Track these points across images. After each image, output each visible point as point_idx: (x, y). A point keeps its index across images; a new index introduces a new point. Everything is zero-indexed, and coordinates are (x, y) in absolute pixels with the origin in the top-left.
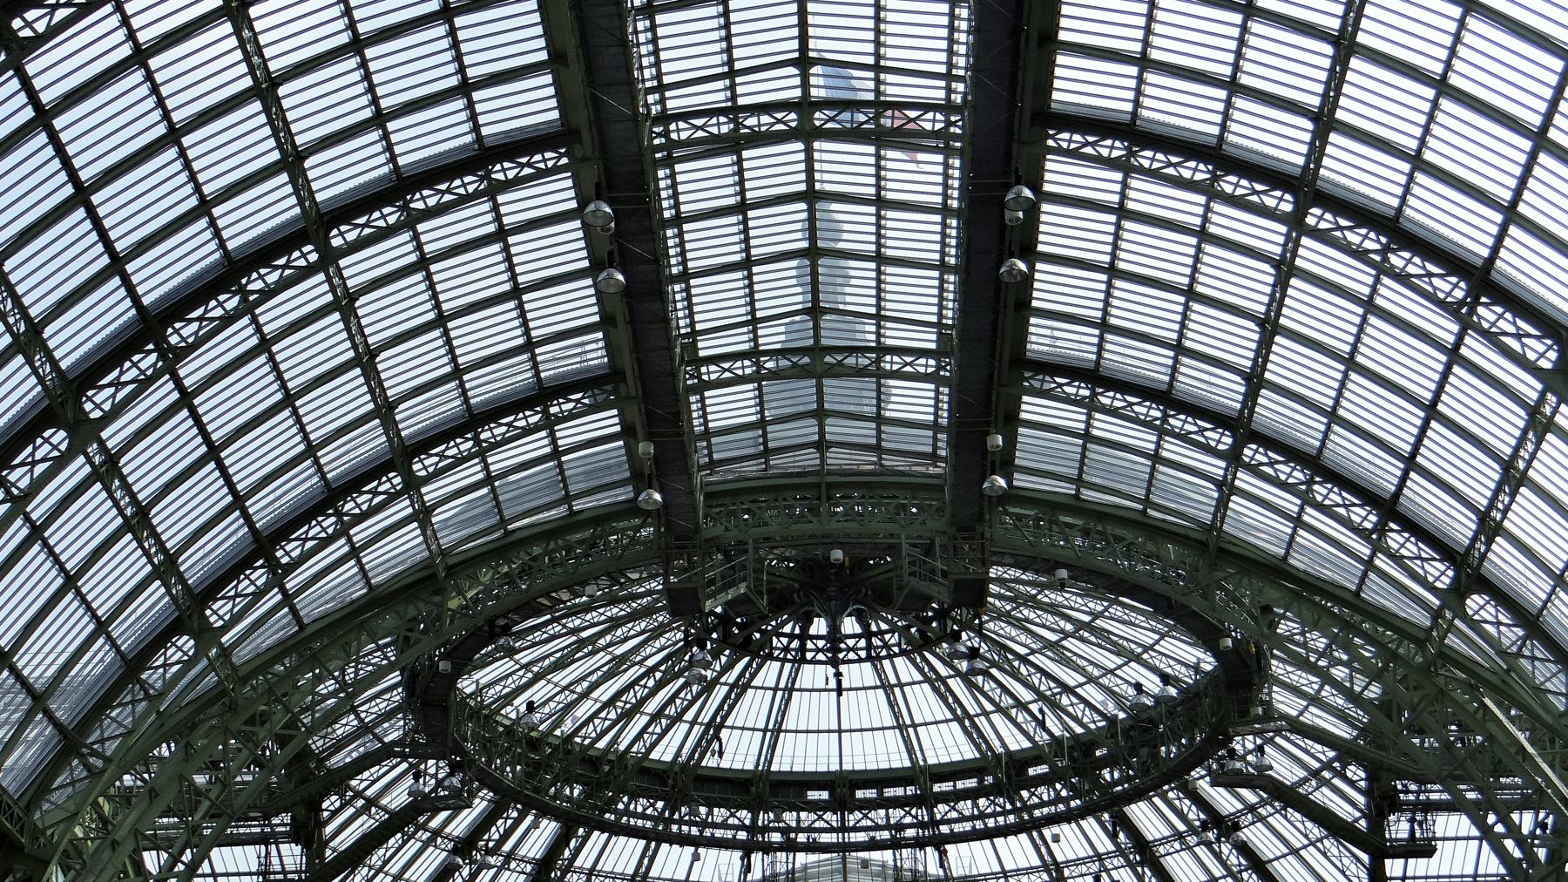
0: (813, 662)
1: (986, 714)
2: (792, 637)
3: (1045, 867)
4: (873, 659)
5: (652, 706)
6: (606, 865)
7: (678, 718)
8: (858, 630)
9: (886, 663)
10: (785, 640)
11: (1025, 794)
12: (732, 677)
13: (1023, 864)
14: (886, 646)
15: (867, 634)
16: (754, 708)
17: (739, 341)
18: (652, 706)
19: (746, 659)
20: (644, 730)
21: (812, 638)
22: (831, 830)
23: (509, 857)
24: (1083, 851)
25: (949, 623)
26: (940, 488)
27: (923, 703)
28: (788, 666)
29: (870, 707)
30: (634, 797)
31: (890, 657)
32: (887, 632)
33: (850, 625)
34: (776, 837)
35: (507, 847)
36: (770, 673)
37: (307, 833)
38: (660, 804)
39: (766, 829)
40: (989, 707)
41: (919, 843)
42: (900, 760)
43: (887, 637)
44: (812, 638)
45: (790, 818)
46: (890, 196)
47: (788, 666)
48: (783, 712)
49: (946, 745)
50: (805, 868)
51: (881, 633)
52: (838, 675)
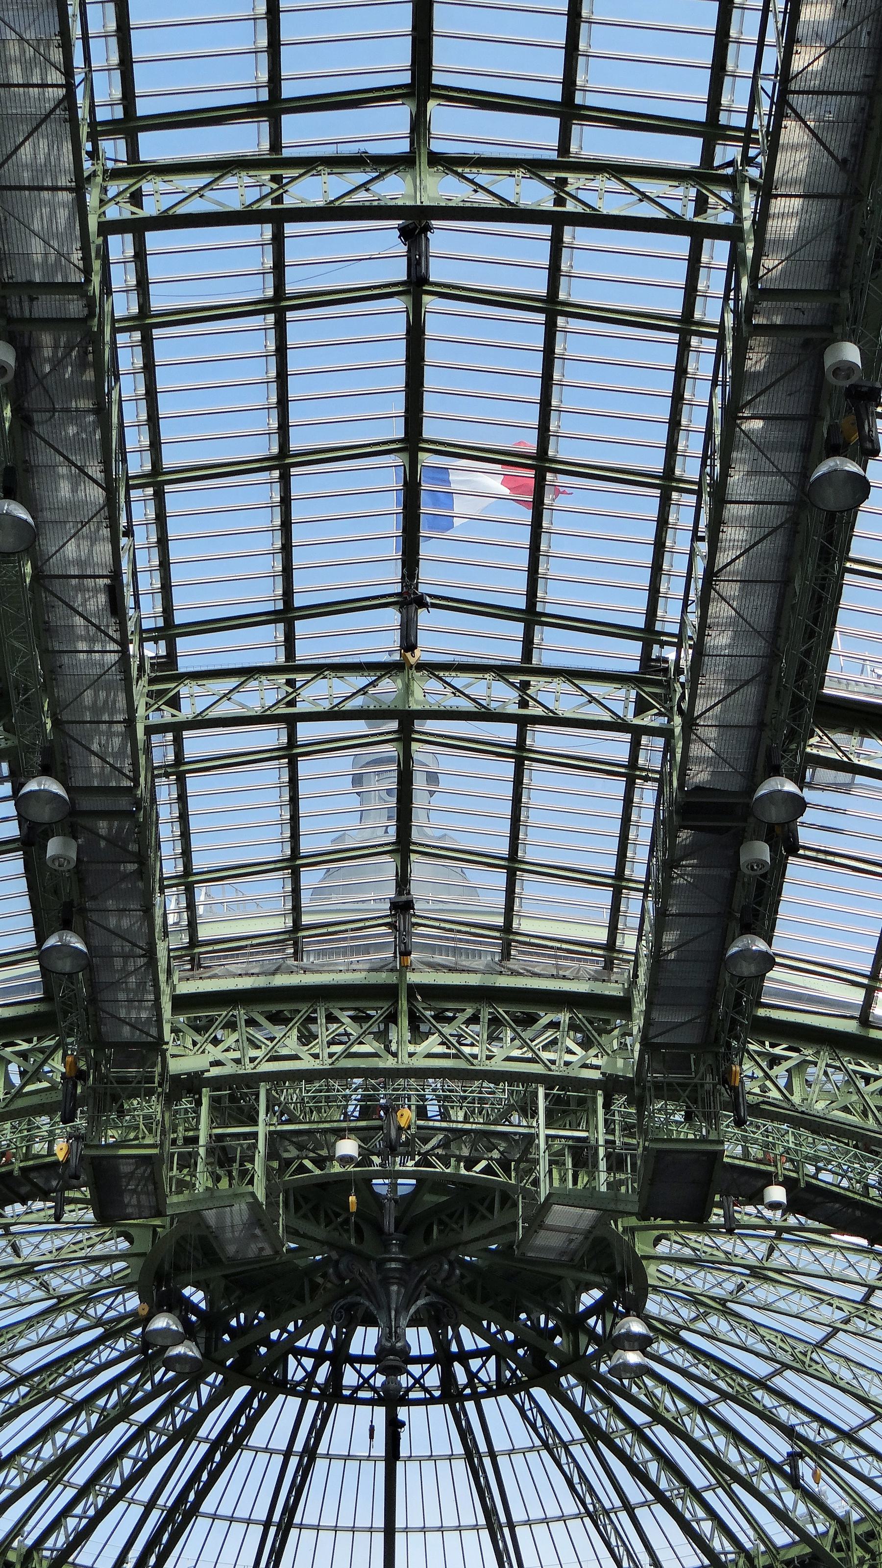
0: (353, 1400)
2: (319, 1356)
4: (449, 1394)
5: (81, 1473)
7: (120, 1494)
8: (428, 1349)
9: (470, 1406)
10: (308, 1362)
12: (212, 1426)
14: (472, 1376)
15: (443, 1357)
17: (261, 645)
18: (82, 1472)
19: (242, 1392)
20: (67, 1511)
21: (355, 1360)
25: (583, 1339)
26: (623, 1006)
28: (312, 1405)
31: (477, 1398)
32: (477, 1353)
33: (420, 1340)
36: (280, 1419)
40: (635, 1492)
44: (355, 1360)
47: (312, 1405)
48: (298, 1489)
51: (464, 1357)
52: (394, 1427)
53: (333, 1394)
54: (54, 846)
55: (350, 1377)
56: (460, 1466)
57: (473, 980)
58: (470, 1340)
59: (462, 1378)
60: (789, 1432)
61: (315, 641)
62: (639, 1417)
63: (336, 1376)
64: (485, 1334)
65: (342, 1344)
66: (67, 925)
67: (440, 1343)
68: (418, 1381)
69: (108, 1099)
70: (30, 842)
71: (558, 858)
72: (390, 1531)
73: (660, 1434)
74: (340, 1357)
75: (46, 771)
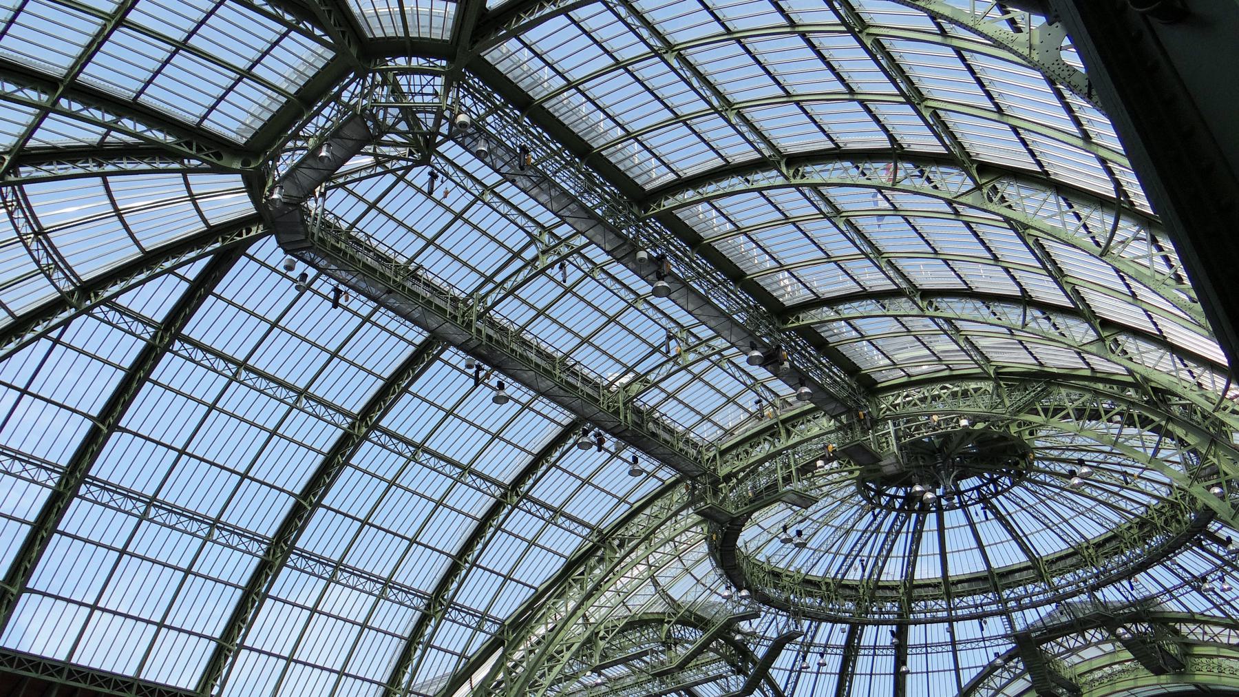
34: (1013, 604)
36: (954, 518)
45: (1020, 590)
50: (1049, 615)
57: (797, 411)
68: (970, 499)
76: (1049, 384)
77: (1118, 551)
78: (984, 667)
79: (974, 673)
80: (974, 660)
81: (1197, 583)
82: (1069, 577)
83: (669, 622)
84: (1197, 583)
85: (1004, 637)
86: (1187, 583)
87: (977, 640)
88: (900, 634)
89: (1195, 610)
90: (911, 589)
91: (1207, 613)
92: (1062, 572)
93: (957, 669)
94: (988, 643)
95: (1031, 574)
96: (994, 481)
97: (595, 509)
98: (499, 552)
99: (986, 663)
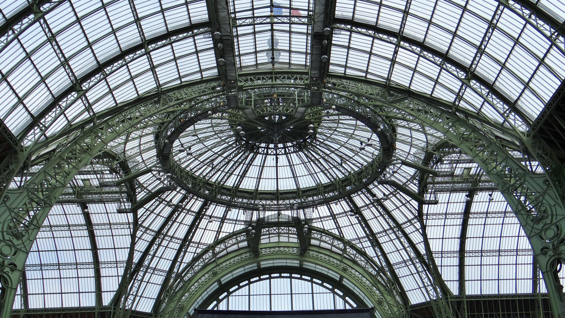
1: (316, 173)
2: (265, 148)
3: (331, 216)
4: (286, 153)
6: (215, 214)
10: (263, 149)
11: (326, 195)
13: (325, 215)
15: (285, 148)
16: (253, 171)
21: (270, 148)
22: (275, 205)
23: (189, 210)
24: (341, 211)
27: (300, 170)
29: (285, 172)
30: (222, 195)
32: (290, 147)
35: (188, 207)
37: (131, 197)
38: (229, 198)
39: (257, 205)
40: (317, 170)
41: (299, 208)
42: (293, 187)
43: (289, 148)
44: (270, 148)
45: (264, 202)
46: (293, 7)
49: (306, 182)
50: (268, 217)
51: (288, 147)
52: (277, 158)
53: (267, 154)
54: (219, 45)
55: (270, 152)
56: (288, 167)
58: (289, 144)
59: (287, 151)
60: (340, 157)
61: (257, 13)
62: (317, 157)
63: (267, 151)
64: (292, 143)
65: (268, 146)
66: (221, 58)
67: (284, 145)
69: (230, 89)
70: (215, 47)
71: (296, 48)
72: (277, 179)
73: (321, 160)
74: (268, 148)
75: (217, 31)
76: (409, 96)
77: (313, 196)
78: (230, 233)
79: (224, 235)
80: (228, 228)
81: (333, 216)
82: (287, 202)
83: (117, 160)
84: (333, 216)
85: (244, 221)
86: (331, 216)
87: (233, 220)
88: (204, 206)
89: (326, 229)
90: (220, 188)
91: (330, 231)
92: (284, 199)
93: (219, 232)
94: (237, 222)
95: (274, 196)
96: (285, 148)
97: (167, 75)
98: (118, 76)
99: (231, 231)
